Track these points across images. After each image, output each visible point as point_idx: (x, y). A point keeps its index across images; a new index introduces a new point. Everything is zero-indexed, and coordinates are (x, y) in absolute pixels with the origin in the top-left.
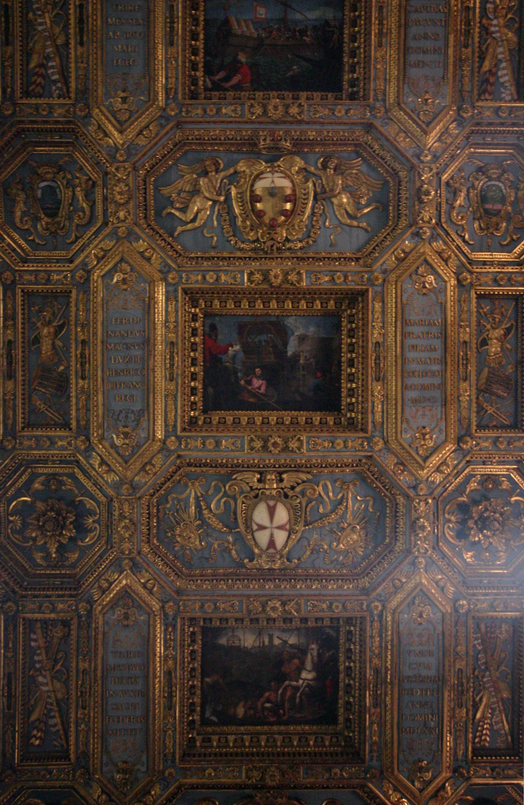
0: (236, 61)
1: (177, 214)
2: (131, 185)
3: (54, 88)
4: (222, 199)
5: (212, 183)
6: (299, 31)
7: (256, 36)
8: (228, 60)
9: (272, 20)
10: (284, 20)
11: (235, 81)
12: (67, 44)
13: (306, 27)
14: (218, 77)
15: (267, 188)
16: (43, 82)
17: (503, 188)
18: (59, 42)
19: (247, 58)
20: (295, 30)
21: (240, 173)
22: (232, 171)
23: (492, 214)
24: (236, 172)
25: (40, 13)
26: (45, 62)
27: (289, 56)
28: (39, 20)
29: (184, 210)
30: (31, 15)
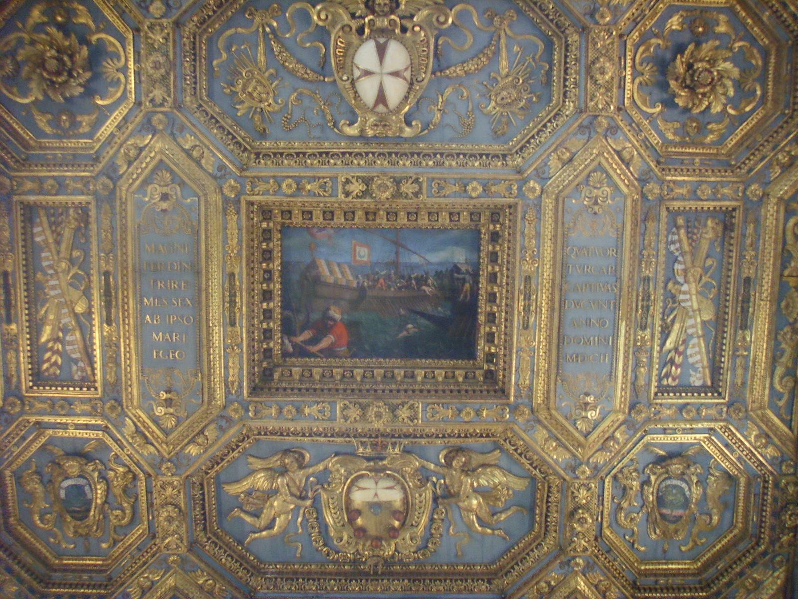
0: (326, 317)
1: (248, 519)
2: (182, 505)
3: (75, 368)
4: (308, 502)
5: (295, 482)
6: (417, 279)
7: (355, 285)
8: (315, 316)
9: (377, 263)
10: (395, 264)
11: (324, 344)
12: (89, 313)
13: (427, 273)
14: (300, 339)
15: (368, 503)
16: (60, 361)
17: (687, 489)
18: (79, 309)
19: (342, 314)
20: (410, 278)
21: (331, 472)
22: (321, 467)
23: (670, 521)
24: (326, 468)
25: (51, 271)
26: (61, 335)
27: (402, 312)
28: (53, 282)
29: (256, 515)
30: (39, 275)
